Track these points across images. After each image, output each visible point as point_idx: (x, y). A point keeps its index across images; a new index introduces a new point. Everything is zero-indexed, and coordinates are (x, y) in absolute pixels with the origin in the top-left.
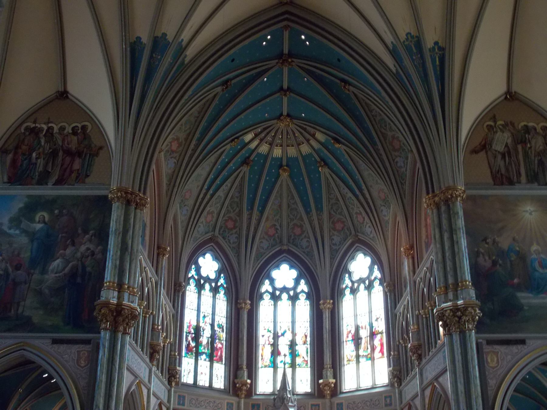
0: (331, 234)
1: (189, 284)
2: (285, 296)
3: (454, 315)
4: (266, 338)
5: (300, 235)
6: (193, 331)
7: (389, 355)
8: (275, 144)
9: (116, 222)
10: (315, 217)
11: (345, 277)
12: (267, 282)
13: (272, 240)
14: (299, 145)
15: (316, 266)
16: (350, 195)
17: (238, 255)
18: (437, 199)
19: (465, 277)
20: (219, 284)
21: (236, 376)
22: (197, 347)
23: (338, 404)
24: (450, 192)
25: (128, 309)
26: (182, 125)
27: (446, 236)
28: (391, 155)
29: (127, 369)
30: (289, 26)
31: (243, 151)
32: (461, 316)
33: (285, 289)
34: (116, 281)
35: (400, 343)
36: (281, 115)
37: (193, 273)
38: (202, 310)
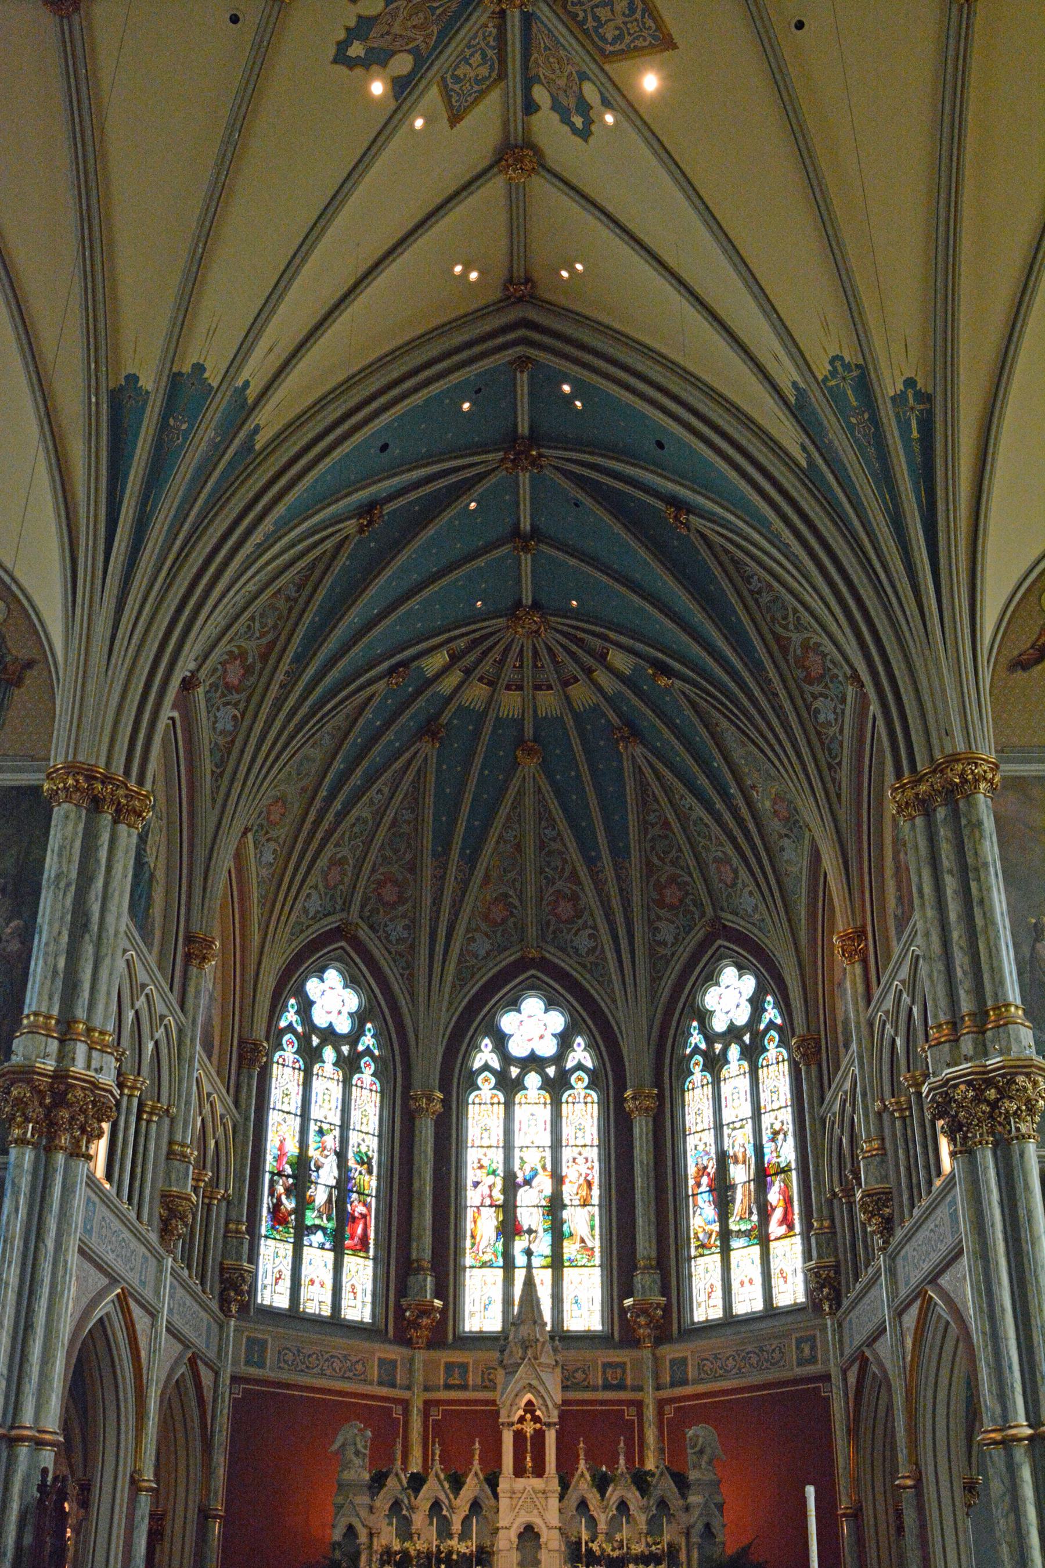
0: (653, 917)
1: (279, 1046)
2: (533, 1080)
3: (978, 1099)
4: (483, 1189)
5: (570, 921)
6: (288, 1170)
7: (807, 1226)
8: (503, 682)
9: (60, 855)
10: (609, 873)
11: (690, 1026)
12: (487, 1044)
13: (499, 934)
14: (566, 684)
15: (614, 1001)
16: (700, 812)
17: (412, 975)
18: (923, 788)
19: (1005, 994)
20: (361, 1048)
21: (402, 1291)
22: (299, 1212)
23: (673, 1362)
24: (959, 767)
25: (83, 1088)
26: (252, 618)
27: (951, 884)
28: (802, 693)
29: (81, 1251)
30: (528, 358)
31: (421, 702)
32: (998, 1100)
33: (533, 1062)
34: (55, 1012)
35: (834, 1195)
36: (518, 604)
37: (290, 1017)
38: (315, 1113)
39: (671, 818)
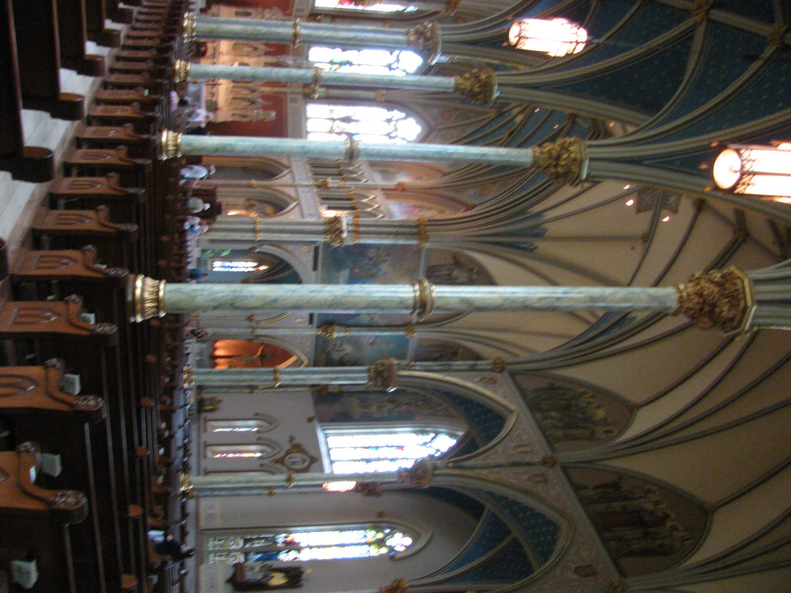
16: (469, 132)
27: (394, 230)
39: (468, 121)
